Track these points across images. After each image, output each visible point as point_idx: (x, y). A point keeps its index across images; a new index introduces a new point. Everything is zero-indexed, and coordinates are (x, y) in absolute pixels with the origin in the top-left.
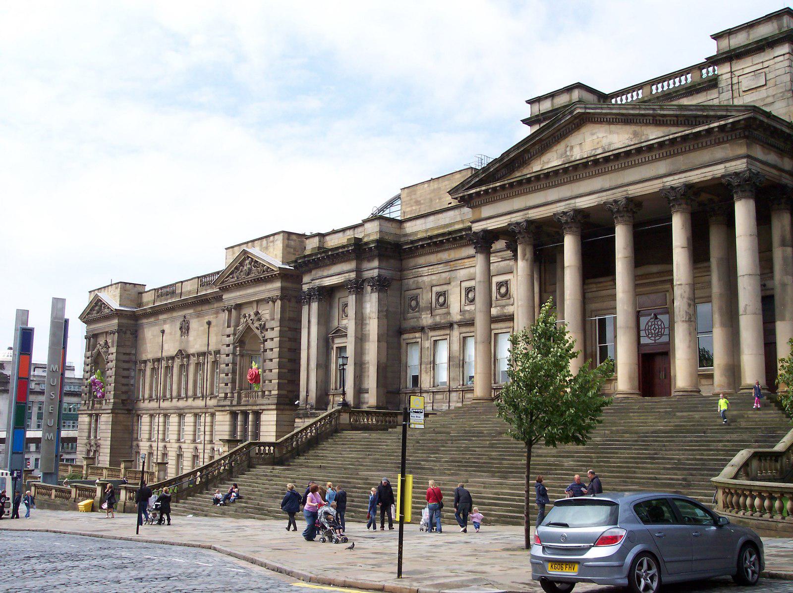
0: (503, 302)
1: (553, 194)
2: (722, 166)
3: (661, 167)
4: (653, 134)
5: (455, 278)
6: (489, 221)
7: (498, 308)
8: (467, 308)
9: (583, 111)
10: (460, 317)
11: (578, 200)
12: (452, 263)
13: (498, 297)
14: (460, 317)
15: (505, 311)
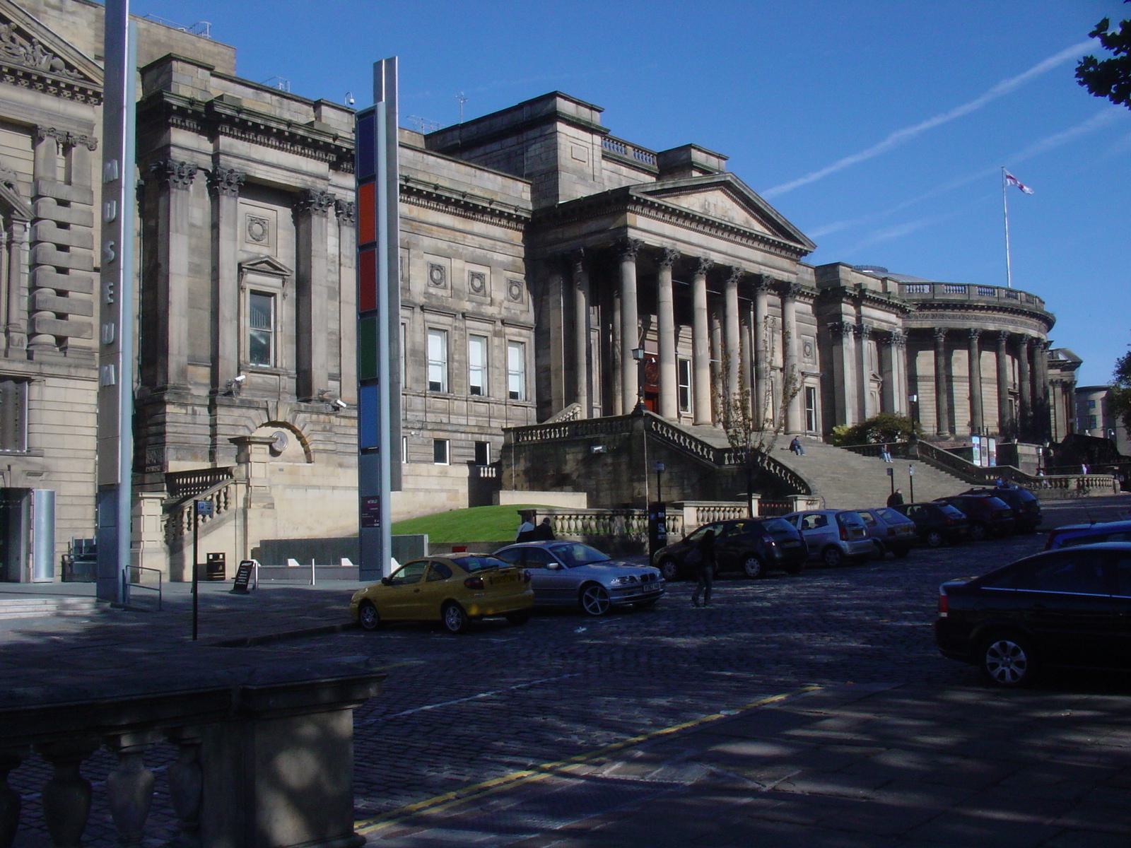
0: (478, 298)
1: (695, 237)
2: (786, 274)
3: (758, 256)
4: (758, 228)
5: (417, 245)
6: (644, 234)
7: (474, 304)
8: (432, 290)
9: (732, 181)
10: (424, 300)
11: (712, 253)
12: (414, 223)
13: (472, 291)
14: (424, 300)
15: (483, 310)
